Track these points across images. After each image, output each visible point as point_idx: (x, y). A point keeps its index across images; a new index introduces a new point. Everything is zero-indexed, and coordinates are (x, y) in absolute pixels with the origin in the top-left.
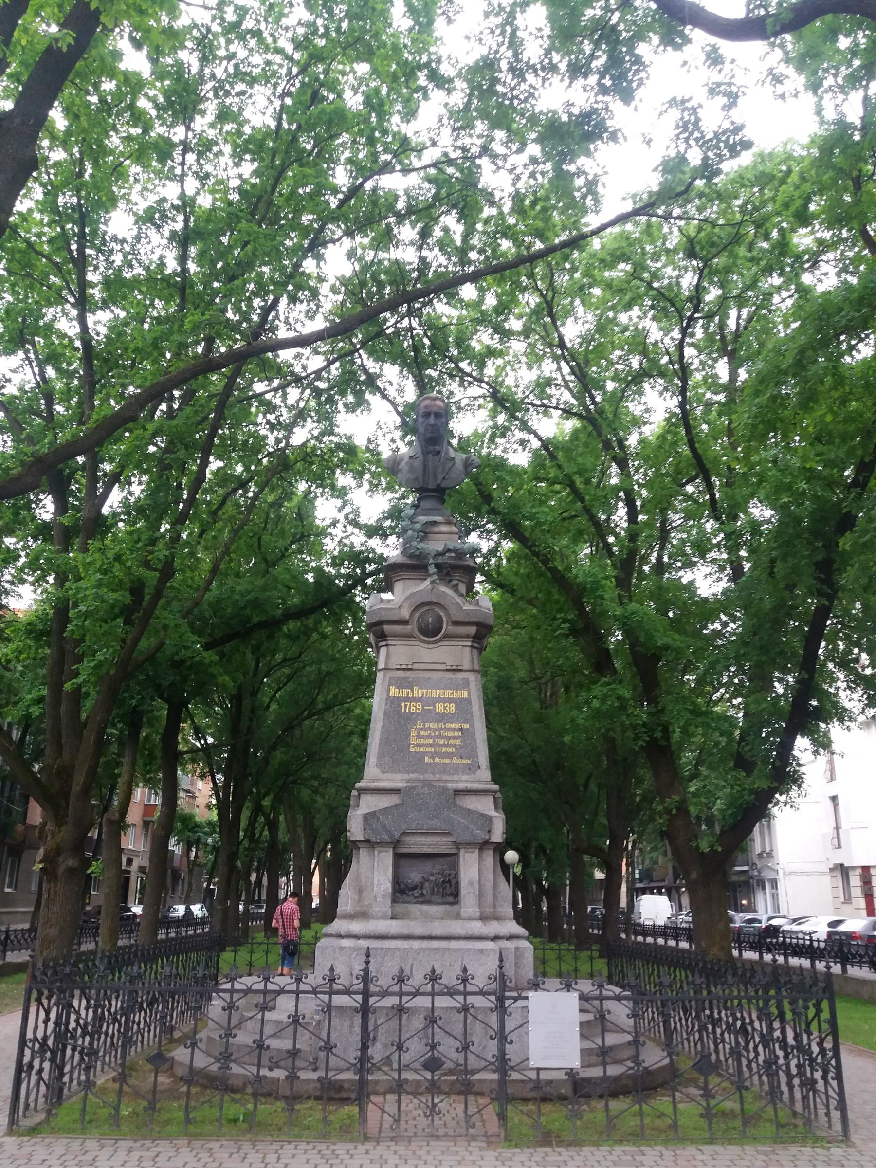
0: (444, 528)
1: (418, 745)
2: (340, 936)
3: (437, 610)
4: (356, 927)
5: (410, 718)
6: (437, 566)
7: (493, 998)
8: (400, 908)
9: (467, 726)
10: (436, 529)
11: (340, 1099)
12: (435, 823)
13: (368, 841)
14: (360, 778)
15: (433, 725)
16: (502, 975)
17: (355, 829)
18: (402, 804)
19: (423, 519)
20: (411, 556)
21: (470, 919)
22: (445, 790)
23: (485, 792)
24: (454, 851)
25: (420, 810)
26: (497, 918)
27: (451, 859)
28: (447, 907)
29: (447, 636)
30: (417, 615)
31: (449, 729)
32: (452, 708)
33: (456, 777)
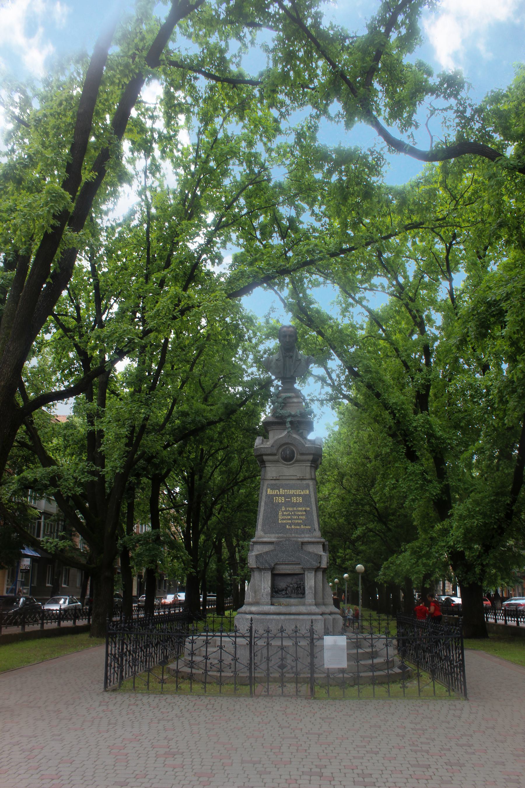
1: (283, 519)
2: (246, 613)
4: (254, 609)
5: (279, 505)
8: (275, 600)
9: (308, 509)
14: (252, 536)
15: (291, 509)
17: (252, 562)
20: (277, 417)
21: (310, 605)
22: (297, 542)
23: (318, 543)
24: (302, 572)
26: (324, 604)
27: (300, 576)
28: (300, 600)
29: (297, 461)
30: (280, 450)
31: (299, 511)
32: (300, 500)
33: (303, 536)
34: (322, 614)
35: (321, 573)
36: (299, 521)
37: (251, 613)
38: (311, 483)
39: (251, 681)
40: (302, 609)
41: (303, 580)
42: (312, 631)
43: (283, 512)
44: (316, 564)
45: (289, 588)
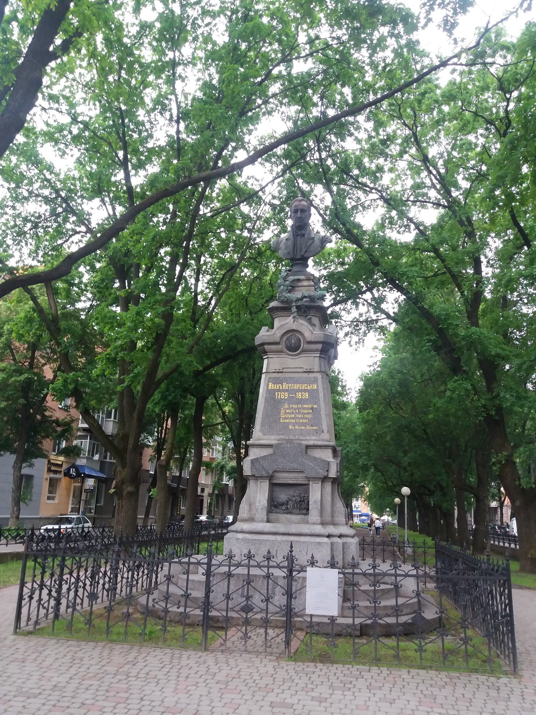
0: (305, 283)
1: (285, 418)
2: (237, 532)
3: (297, 335)
4: (246, 526)
5: (281, 402)
6: (298, 307)
7: (285, 570)
8: (273, 516)
9: (315, 406)
10: (300, 284)
11: (207, 625)
12: (295, 466)
13: (254, 476)
15: (295, 406)
16: (292, 556)
18: (274, 453)
19: (291, 278)
20: (282, 302)
21: (314, 524)
22: (300, 445)
24: (306, 482)
25: (284, 458)
26: (334, 524)
27: (305, 487)
29: (304, 351)
30: (285, 338)
31: (305, 408)
32: (306, 395)
34: (329, 536)
35: (330, 483)
36: (305, 421)
37: (242, 532)
38: (319, 376)
39: (222, 625)
40: (305, 529)
41: (307, 492)
42: (290, 558)
43: (285, 409)
44: (323, 473)
45: (290, 502)
